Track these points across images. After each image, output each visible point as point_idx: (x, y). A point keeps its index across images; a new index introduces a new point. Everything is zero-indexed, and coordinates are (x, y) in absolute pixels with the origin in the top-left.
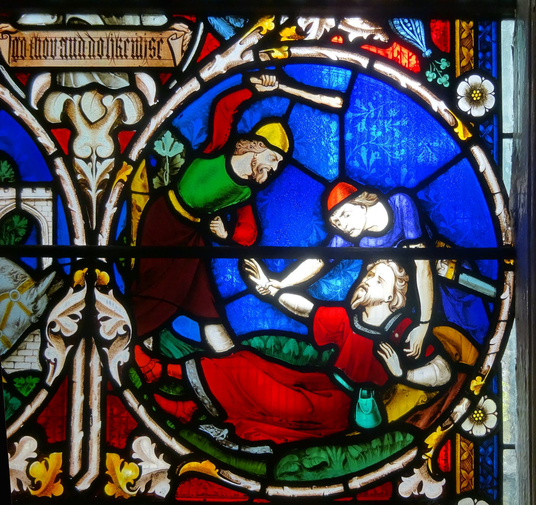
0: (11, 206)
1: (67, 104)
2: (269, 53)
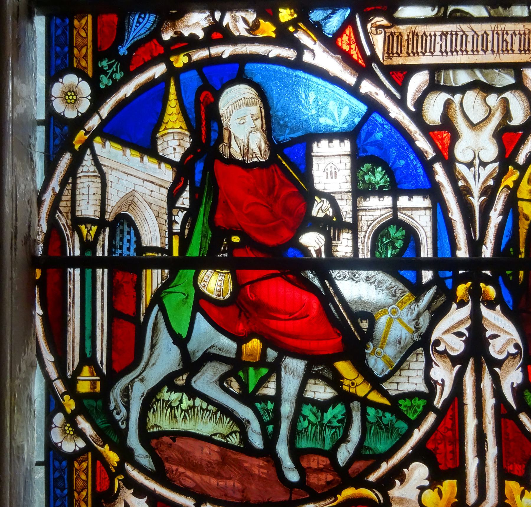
0: (387, 215)
1: (448, 104)
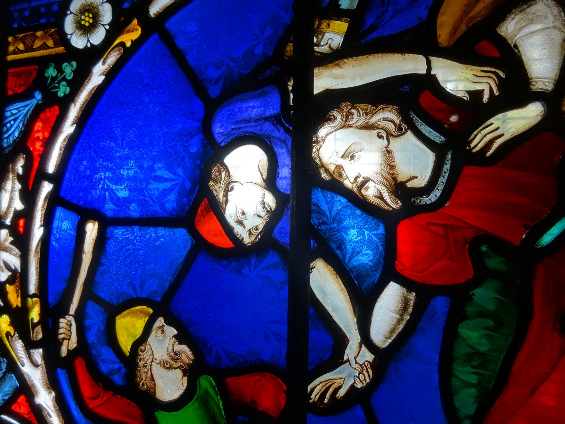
2: (35, 325)
